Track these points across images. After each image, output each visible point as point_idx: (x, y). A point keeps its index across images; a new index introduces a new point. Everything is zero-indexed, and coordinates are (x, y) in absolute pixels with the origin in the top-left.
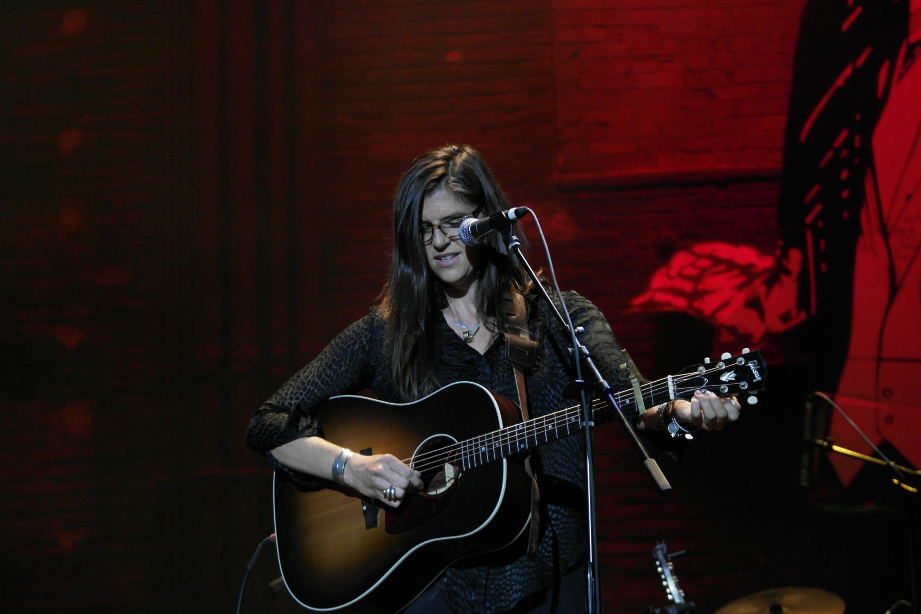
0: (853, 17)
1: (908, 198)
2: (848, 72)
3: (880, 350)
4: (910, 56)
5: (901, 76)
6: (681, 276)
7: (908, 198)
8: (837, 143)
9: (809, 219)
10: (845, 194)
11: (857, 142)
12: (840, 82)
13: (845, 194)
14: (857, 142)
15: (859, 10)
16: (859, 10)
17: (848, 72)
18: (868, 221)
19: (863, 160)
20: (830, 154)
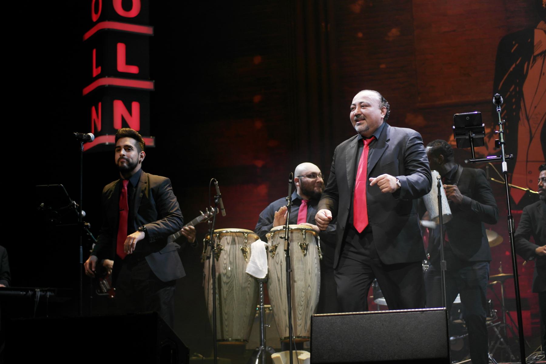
1: (535, 107)
2: (514, 66)
4: (535, 60)
5: (532, 67)
7: (535, 107)
10: (514, 107)
12: (511, 69)
13: (514, 107)
15: (517, 45)
16: (517, 45)
17: (514, 66)
18: (522, 115)
19: (520, 95)
20: (509, 94)
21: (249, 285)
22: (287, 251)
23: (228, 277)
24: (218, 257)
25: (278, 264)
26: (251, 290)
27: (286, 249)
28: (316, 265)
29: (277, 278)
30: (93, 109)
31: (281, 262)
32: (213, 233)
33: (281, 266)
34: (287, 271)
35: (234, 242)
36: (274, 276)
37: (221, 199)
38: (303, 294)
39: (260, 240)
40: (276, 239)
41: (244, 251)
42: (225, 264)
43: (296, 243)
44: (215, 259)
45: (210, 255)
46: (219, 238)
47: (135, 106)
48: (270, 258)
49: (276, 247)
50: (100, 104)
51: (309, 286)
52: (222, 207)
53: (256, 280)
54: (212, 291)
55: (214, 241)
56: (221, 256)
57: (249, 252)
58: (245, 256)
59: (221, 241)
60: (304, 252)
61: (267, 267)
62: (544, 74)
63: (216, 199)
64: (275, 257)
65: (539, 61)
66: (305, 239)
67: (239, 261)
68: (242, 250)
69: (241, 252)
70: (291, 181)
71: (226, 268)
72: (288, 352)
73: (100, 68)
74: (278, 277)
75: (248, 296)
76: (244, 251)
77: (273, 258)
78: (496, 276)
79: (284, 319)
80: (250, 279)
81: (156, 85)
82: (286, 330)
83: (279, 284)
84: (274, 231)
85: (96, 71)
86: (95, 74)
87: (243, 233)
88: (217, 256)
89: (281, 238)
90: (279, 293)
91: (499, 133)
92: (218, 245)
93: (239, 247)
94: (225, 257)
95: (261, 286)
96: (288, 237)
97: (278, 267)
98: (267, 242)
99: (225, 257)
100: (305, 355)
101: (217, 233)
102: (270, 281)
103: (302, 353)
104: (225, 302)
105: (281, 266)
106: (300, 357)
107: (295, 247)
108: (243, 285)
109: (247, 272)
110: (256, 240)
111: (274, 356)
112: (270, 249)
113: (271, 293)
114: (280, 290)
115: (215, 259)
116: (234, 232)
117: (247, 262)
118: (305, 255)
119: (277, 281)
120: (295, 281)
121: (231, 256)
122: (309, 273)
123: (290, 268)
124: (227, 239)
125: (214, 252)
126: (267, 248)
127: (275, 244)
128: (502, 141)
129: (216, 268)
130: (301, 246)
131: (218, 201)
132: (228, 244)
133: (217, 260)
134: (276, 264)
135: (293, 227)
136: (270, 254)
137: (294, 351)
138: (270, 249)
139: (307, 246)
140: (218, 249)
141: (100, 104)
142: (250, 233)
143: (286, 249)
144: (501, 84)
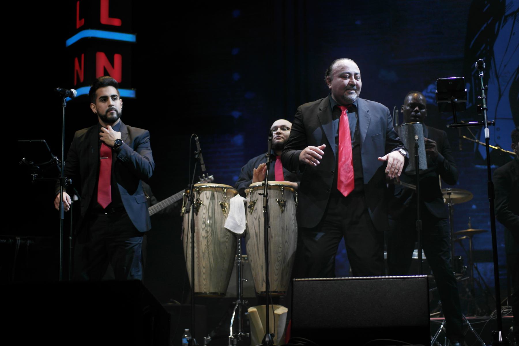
0: (486, 8)
1: (505, 66)
2: (485, 25)
3: (496, 117)
4: (506, 20)
5: (503, 27)
6: (431, 92)
7: (505, 66)
8: (482, 49)
9: (473, 73)
11: (488, 48)
12: (483, 28)
14: (488, 48)
17: (485, 25)
20: (480, 52)
21: (227, 240)
22: (266, 207)
23: (207, 232)
24: (198, 211)
25: (256, 219)
26: (229, 245)
27: (265, 205)
28: (294, 222)
29: (254, 234)
30: (76, 60)
31: (259, 218)
32: (193, 187)
33: (259, 222)
34: (265, 227)
35: (213, 196)
36: (252, 232)
37: (201, 154)
38: (280, 250)
39: (238, 195)
40: (254, 195)
41: (223, 206)
42: (204, 218)
43: (275, 199)
44: (195, 214)
45: (190, 209)
46: (199, 193)
47: (118, 59)
48: (249, 214)
49: (255, 203)
50: (83, 56)
51: (286, 242)
52: (202, 162)
53: (234, 235)
54: (190, 245)
55: (194, 196)
56: (200, 210)
57: (227, 207)
58: (223, 211)
59: (201, 195)
60: (281, 208)
61: (245, 222)
62: (514, 34)
63: (196, 154)
64: (253, 213)
65: (510, 21)
66: (282, 196)
67: (218, 216)
68: (221, 205)
69: (220, 206)
70: (270, 138)
71: (204, 223)
72: (264, 306)
73: (83, 20)
74: (256, 233)
75: (226, 251)
76: (223, 206)
77: (251, 213)
78: (465, 231)
79: (261, 274)
80: (228, 234)
81: (137, 38)
82: (262, 285)
83: (257, 240)
84: (253, 187)
85: (79, 23)
86: (78, 26)
87: (222, 188)
88: (196, 210)
89: (260, 194)
90: (256, 248)
91: (482, 99)
92: (197, 200)
93: (217, 203)
94: (204, 211)
95: (239, 241)
96: (267, 194)
97: (256, 222)
98: (246, 198)
99: (204, 211)
100: (282, 310)
101: (196, 187)
102: (248, 236)
103: (278, 308)
104: (203, 256)
105: (259, 222)
106: (276, 312)
107: (273, 203)
108: (222, 240)
109: (225, 227)
110: (235, 195)
111: (251, 309)
112: (248, 204)
113: (249, 248)
114: (257, 245)
115: (195, 214)
116: (214, 187)
117: (226, 217)
118: (283, 212)
119: (255, 236)
120: (272, 237)
121: (210, 211)
122: (287, 229)
123: (268, 224)
124: (206, 194)
125: (193, 206)
126: (245, 203)
127: (253, 199)
128: (485, 106)
129: (195, 222)
130: (279, 202)
131: (199, 156)
132: (207, 198)
133: (197, 214)
134: (254, 219)
135: (272, 183)
136: (248, 210)
137: (270, 306)
138: (248, 204)
139: (285, 202)
140: (197, 203)
141: (83, 56)
142: (229, 188)
143: (265, 205)
144: (472, 43)
